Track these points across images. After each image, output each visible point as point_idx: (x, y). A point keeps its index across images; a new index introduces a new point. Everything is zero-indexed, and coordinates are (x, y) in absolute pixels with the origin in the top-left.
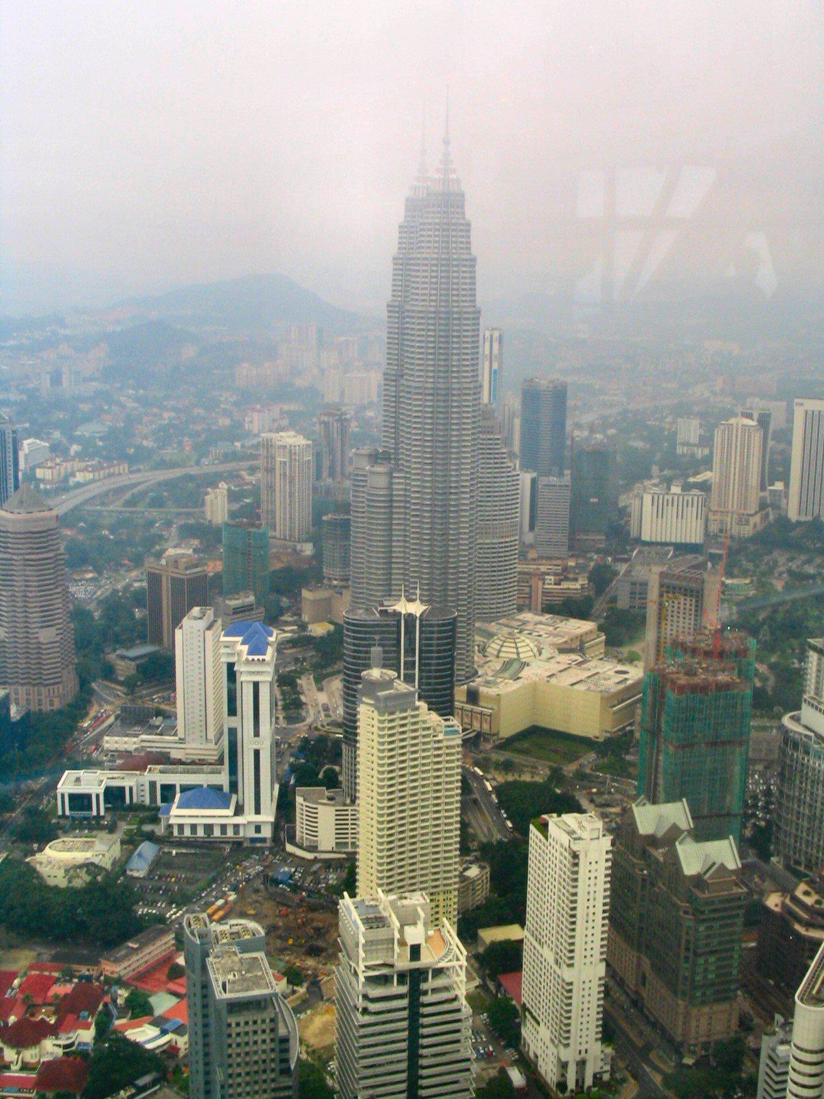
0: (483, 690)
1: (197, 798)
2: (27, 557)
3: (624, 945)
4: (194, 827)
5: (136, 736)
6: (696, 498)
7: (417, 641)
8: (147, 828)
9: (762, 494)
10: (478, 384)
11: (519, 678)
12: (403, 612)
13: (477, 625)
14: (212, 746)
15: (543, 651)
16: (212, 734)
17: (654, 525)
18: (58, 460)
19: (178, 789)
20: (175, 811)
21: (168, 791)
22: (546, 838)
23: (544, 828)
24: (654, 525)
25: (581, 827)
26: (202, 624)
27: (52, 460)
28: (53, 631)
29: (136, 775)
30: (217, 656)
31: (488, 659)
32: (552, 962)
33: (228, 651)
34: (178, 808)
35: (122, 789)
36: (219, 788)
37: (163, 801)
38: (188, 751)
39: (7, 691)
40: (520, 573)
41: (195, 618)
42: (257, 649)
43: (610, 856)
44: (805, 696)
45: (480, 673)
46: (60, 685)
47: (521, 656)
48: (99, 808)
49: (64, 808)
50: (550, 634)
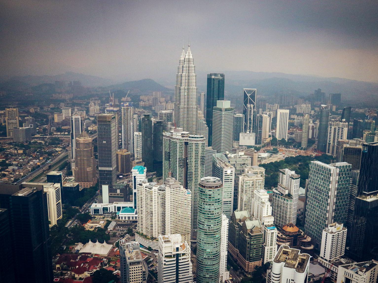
2: (84, 149)
4: (125, 217)
9: (269, 133)
18: (94, 125)
20: (120, 213)
21: (119, 209)
27: (92, 125)
28: (90, 168)
34: (121, 213)
35: (107, 208)
36: (132, 207)
39: (78, 183)
46: (92, 182)
48: (101, 212)
49: (92, 213)
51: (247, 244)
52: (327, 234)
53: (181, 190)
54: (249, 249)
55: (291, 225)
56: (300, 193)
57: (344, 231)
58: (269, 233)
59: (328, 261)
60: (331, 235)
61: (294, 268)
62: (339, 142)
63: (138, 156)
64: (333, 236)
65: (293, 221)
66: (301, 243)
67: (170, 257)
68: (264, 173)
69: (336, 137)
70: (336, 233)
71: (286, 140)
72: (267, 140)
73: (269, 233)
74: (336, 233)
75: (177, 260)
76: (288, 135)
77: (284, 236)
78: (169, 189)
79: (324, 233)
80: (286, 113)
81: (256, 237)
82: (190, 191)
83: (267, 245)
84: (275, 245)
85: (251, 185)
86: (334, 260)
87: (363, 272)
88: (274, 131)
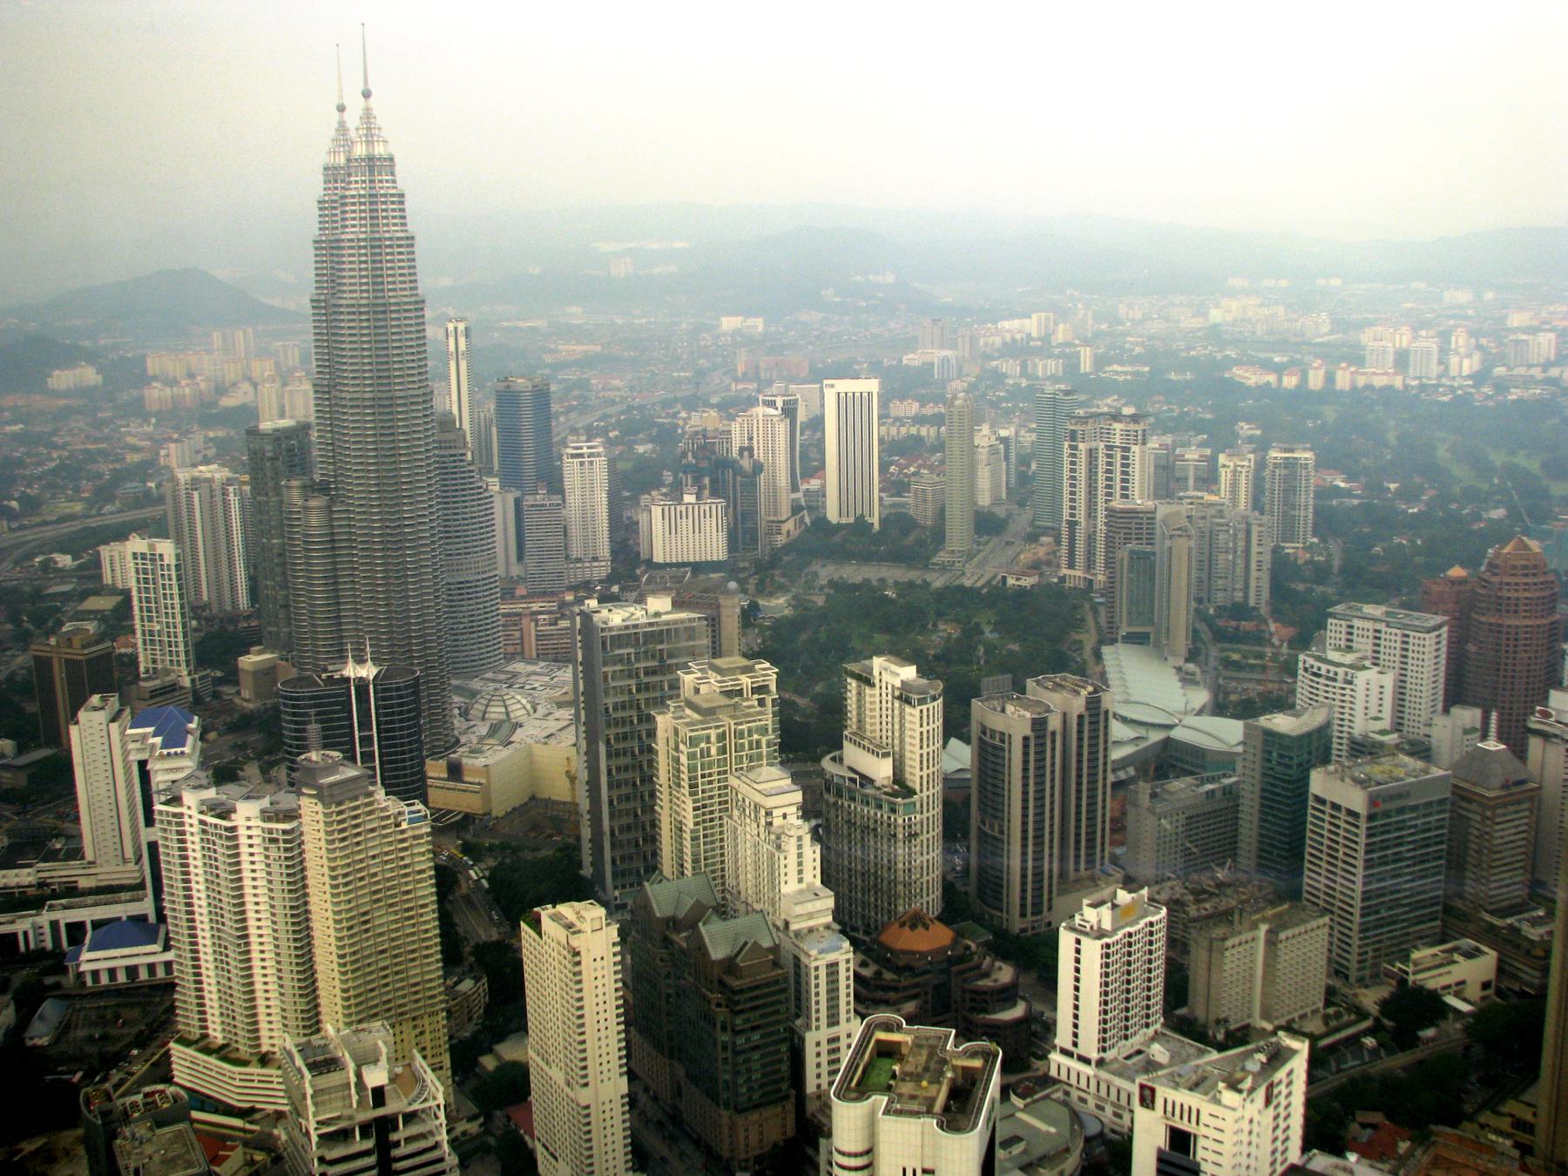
0: (467, 762)
1: (110, 933)
3: (654, 1053)
4: (112, 972)
5: (30, 866)
6: (714, 506)
7: (373, 711)
8: (49, 980)
9: (794, 496)
10: (428, 390)
11: (511, 743)
12: (352, 676)
13: (454, 682)
14: (131, 866)
15: (539, 707)
16: (129, 853)
17: (667, 542)
19: (89, 926)
20: (85, 956)
21: (76, 930)
22: (540, 934)
23: (536, 924)
24: (667, 542)
25: (580, 918)
26: (101, 716)
29: (32, 916)
30: (126, 753)
31: (472, 723)
32: (562, 1083)
33: (138, 745)
34: (90, 950)
35: (15, 935)
36: (143, 919)
37: (69, 945)
38: (100, 877)
40: (504, 615)
41: (95, 709)
42: (174, 739)
43: (618, 949)
44: (846, 733)
45: (463, 740)
47: (512, 715)
50: (546, 686)
51: (719, 1028)
52: (1078, 942)
53: (376, 806)
54: (729, 1054)
55: (916, 921)
56: (951, 766)
57: (1153, 919)
58: (817, 968)
59: (1093, 1063)
60: (1099, 943)
61: (929, 1112)
62: (1111, 513)
63: (154, 661)
64: (1108, 946)
65: (930, 900)
66: (968, 996)
67: (345, 1135)
68: (773, 687)
69: (1101, 491)
70: (1120, 934)
71: (875, 520)
72: (785, 527)
73: (817, 968)
74: (1120, 934)
75: (384, 1148)
76: (881, 499)
77: (888, 976)
78: (320, 808)
79: (1066, 940)
80: (865, 395)
81: (757, 992)
82: (421, 807)
83: (814, 1024)
84: (848, 1020)
85: (713, 751)
86: (1120, 1058)
87: (1240, 1091)
88: (814, 484)
